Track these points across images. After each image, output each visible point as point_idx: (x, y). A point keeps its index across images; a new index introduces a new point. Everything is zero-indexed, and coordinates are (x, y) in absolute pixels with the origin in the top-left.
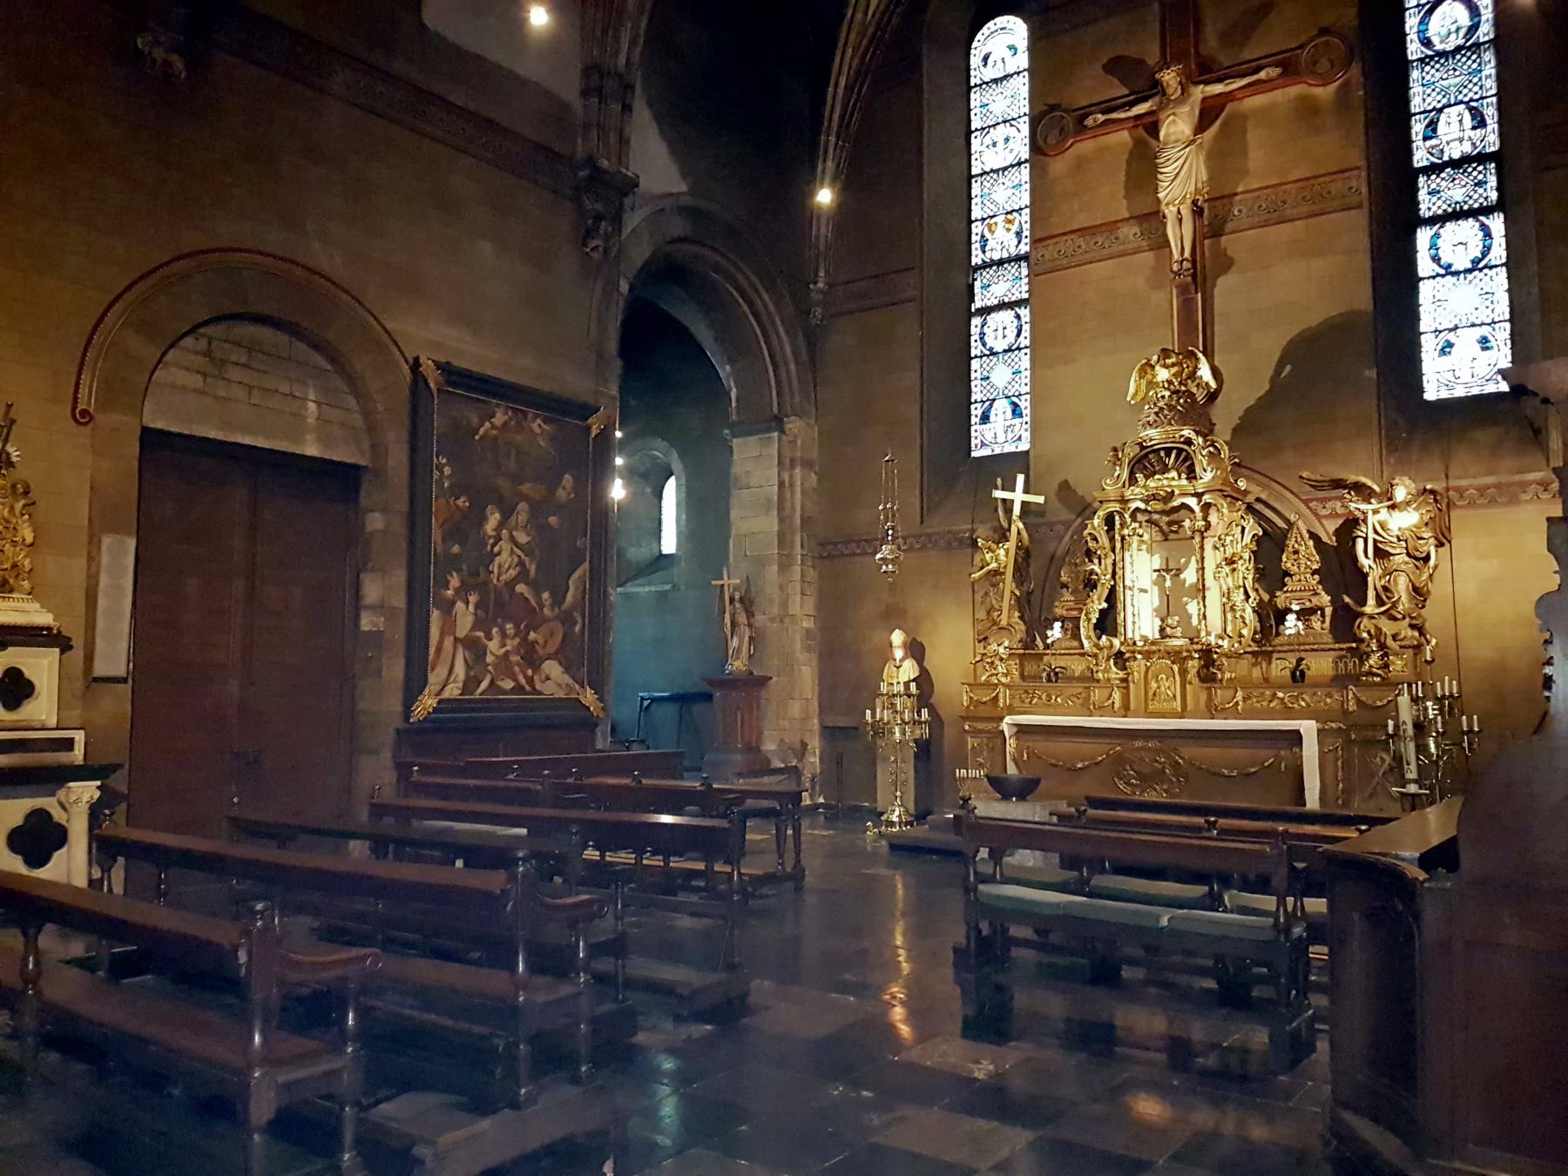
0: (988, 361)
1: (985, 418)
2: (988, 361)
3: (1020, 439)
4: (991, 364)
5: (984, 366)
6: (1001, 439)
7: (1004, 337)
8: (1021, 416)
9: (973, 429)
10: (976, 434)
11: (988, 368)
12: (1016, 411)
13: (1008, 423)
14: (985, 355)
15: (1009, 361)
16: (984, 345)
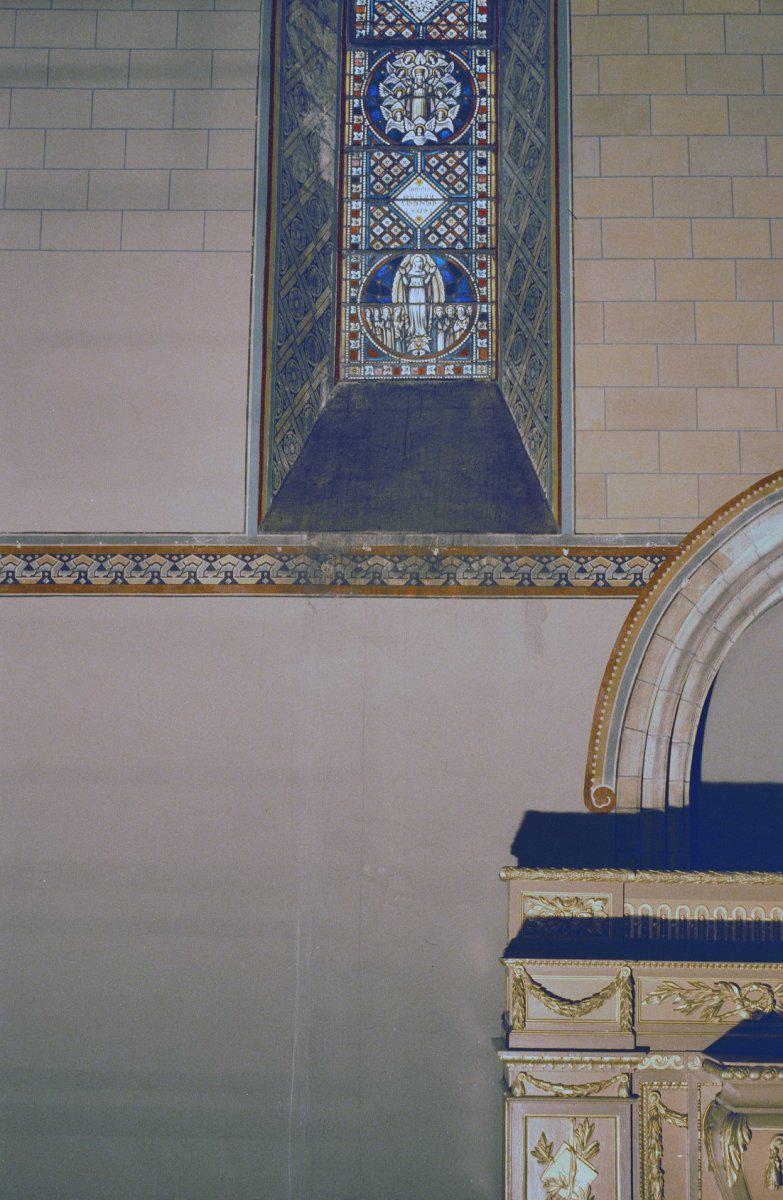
0: (388, 162)
1: (377, 292)
2: (388, 162)
3: (466, 352)
4: (396, 171)
5: (378, 170)
6: (419, 345)
7: (428, 115)
8: (469, 298)
9: (345, 312)
10: (354, 327)
11: (387, 178)
12: (458, 286)
13: (439, 312)
14: (379, 146)
15: (442, 170)
16: (379, 123)
